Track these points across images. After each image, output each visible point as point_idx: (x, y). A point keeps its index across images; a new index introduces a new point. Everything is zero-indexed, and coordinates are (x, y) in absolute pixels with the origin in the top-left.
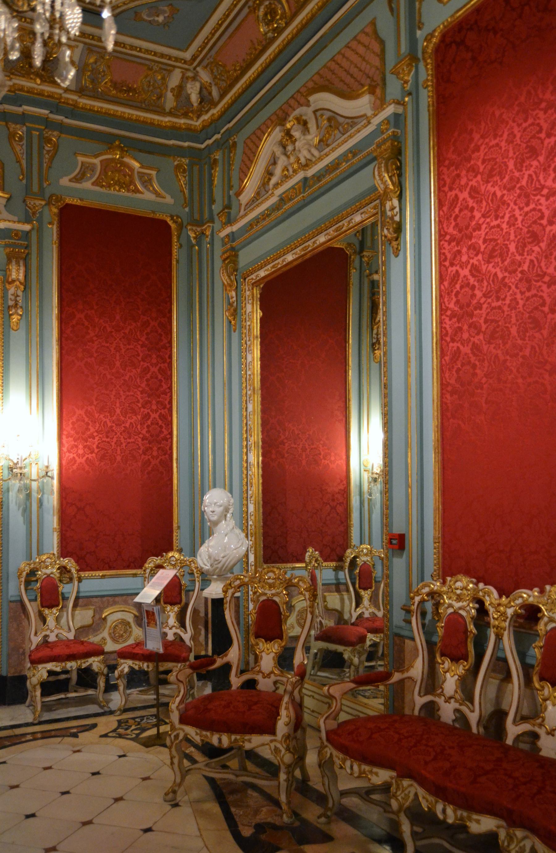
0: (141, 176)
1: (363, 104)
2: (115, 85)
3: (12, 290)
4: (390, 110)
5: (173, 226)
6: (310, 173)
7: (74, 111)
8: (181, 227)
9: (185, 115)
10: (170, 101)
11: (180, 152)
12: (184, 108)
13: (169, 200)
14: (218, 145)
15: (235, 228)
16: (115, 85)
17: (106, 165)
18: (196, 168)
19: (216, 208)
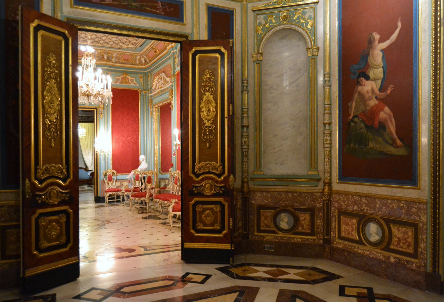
0: (131, 80)
1: (168, 79)
2: (124, 60)
3: (101, 110)
4: (171, 84)
5: (139, 91)
6: (162, 89)
7: (114, 67)
8: (141, 91)
9: (141, 65)
10: (138, 62)
11: (141, 73)
12: (141, 63)
13: (138, 85)
14: (149, 72)
15: (152, 94)
16: (124, 60)
17: (122, 78)
18: (145, 77)
19: (149, 87)
